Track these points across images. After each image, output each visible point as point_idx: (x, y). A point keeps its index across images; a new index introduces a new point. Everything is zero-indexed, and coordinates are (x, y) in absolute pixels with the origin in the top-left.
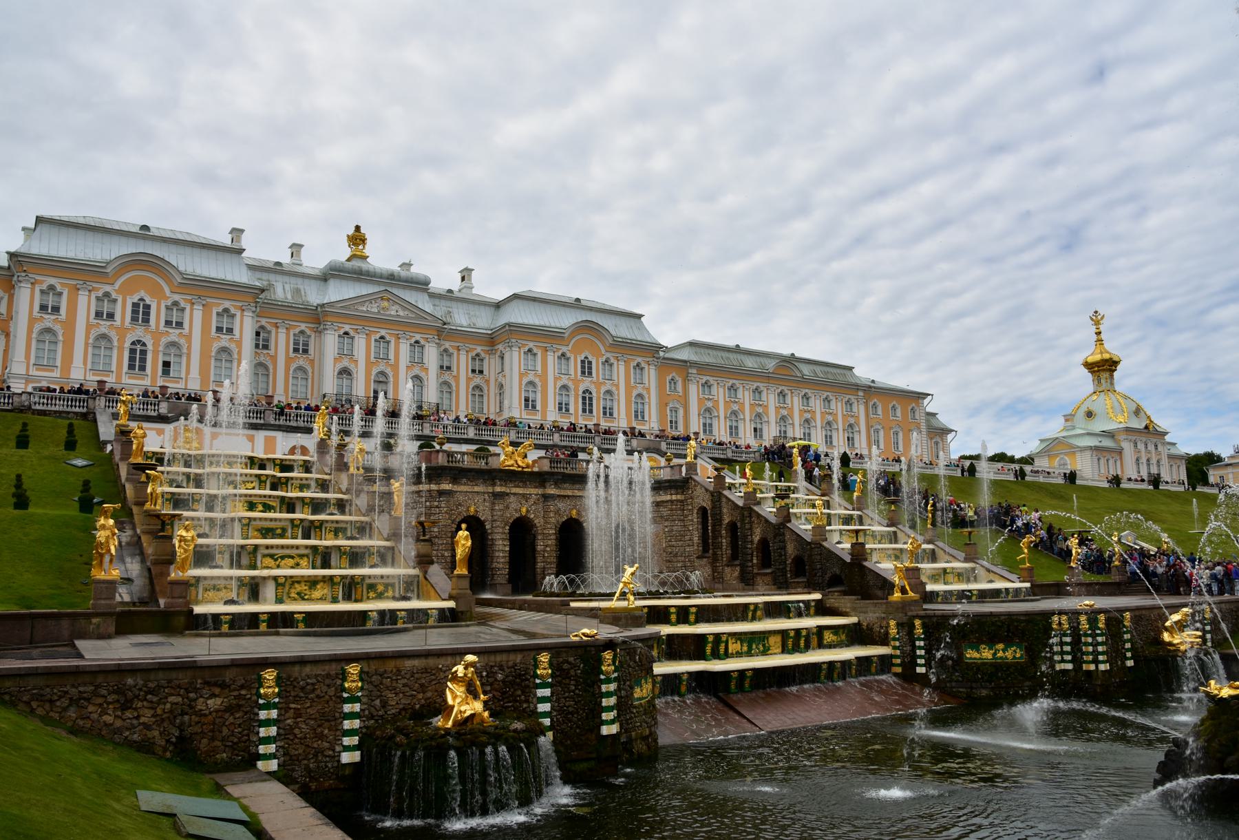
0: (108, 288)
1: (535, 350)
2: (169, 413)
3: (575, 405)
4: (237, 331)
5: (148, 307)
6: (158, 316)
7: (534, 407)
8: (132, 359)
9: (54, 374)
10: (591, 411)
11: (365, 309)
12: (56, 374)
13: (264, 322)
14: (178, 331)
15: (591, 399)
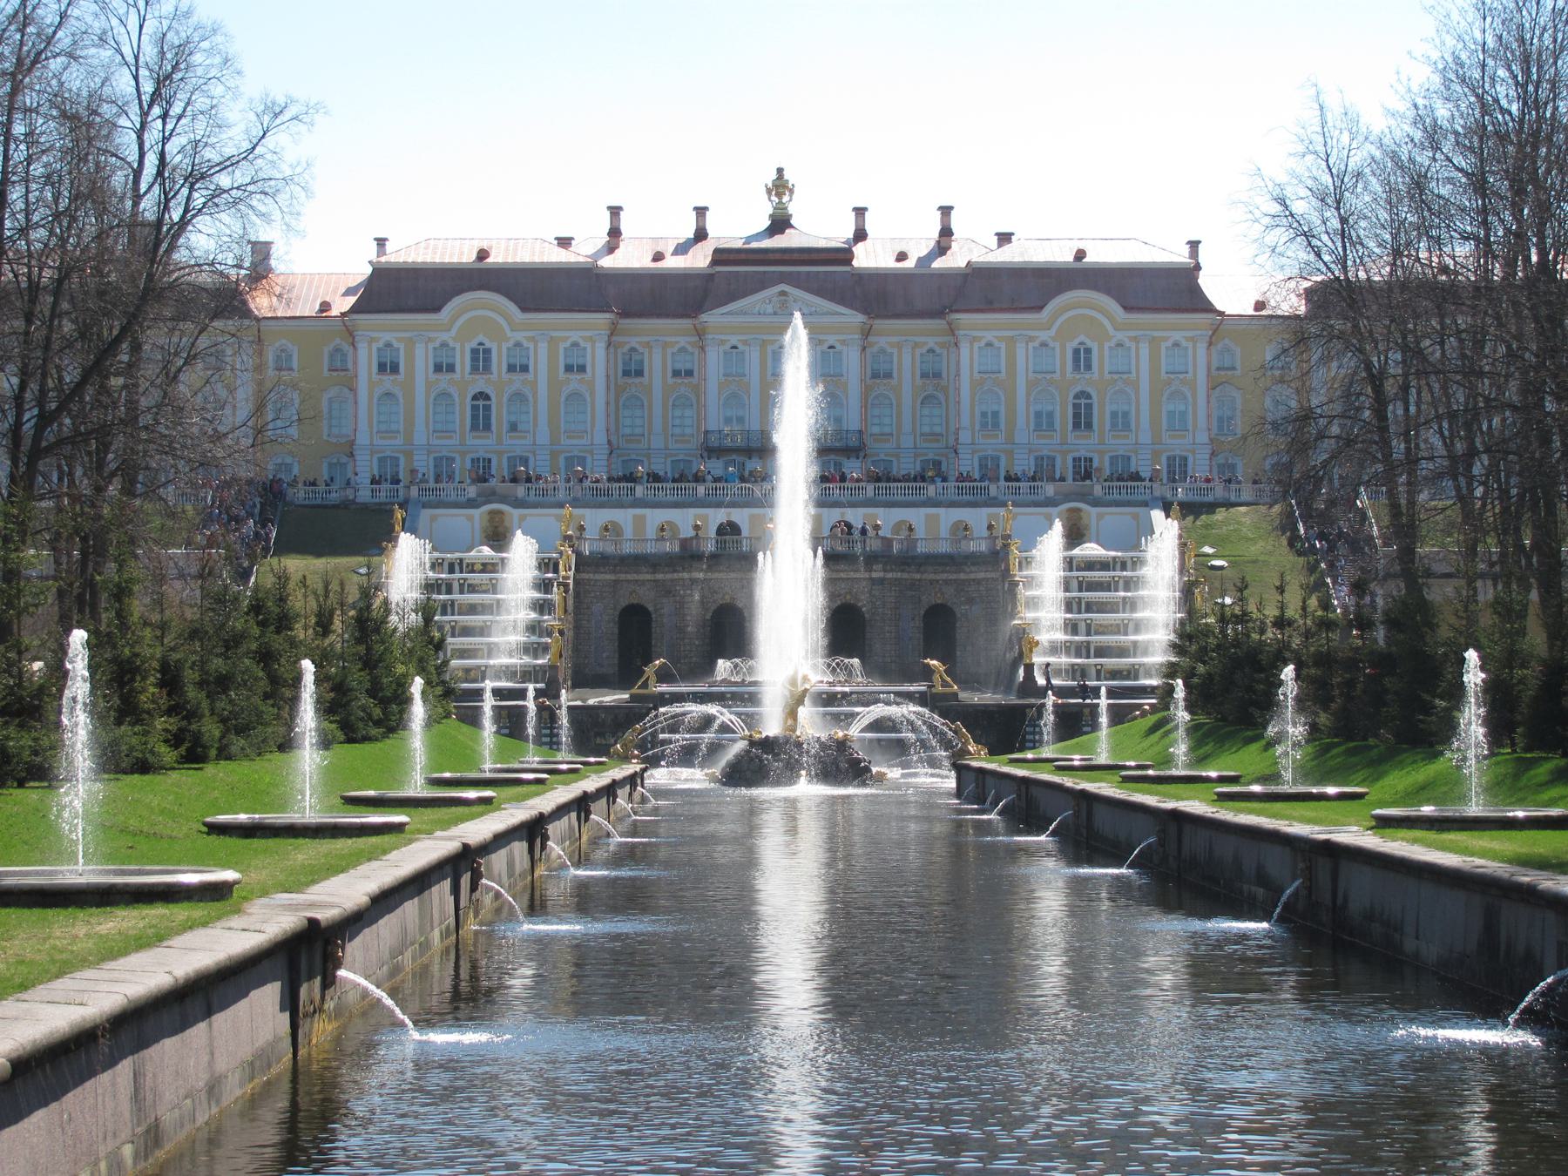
0: (445, 337)
1: (996, 343)
2: (478, 495)
3: (1063, 415)
4: (589, 369)
5: (487, 351)
6: (499, 362)
7: (996, 425)
8: (475, 417)
9: (397, 442)
10: (1089, 426)
11: (756, 311)
12: (399, 441)
13: (634, 345)
14: (523, 376)
15: (1089, 407)
